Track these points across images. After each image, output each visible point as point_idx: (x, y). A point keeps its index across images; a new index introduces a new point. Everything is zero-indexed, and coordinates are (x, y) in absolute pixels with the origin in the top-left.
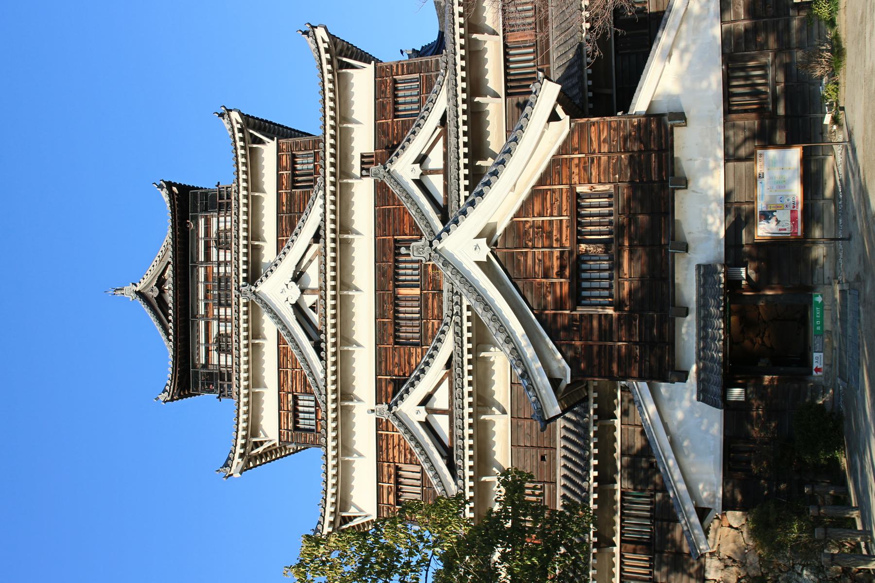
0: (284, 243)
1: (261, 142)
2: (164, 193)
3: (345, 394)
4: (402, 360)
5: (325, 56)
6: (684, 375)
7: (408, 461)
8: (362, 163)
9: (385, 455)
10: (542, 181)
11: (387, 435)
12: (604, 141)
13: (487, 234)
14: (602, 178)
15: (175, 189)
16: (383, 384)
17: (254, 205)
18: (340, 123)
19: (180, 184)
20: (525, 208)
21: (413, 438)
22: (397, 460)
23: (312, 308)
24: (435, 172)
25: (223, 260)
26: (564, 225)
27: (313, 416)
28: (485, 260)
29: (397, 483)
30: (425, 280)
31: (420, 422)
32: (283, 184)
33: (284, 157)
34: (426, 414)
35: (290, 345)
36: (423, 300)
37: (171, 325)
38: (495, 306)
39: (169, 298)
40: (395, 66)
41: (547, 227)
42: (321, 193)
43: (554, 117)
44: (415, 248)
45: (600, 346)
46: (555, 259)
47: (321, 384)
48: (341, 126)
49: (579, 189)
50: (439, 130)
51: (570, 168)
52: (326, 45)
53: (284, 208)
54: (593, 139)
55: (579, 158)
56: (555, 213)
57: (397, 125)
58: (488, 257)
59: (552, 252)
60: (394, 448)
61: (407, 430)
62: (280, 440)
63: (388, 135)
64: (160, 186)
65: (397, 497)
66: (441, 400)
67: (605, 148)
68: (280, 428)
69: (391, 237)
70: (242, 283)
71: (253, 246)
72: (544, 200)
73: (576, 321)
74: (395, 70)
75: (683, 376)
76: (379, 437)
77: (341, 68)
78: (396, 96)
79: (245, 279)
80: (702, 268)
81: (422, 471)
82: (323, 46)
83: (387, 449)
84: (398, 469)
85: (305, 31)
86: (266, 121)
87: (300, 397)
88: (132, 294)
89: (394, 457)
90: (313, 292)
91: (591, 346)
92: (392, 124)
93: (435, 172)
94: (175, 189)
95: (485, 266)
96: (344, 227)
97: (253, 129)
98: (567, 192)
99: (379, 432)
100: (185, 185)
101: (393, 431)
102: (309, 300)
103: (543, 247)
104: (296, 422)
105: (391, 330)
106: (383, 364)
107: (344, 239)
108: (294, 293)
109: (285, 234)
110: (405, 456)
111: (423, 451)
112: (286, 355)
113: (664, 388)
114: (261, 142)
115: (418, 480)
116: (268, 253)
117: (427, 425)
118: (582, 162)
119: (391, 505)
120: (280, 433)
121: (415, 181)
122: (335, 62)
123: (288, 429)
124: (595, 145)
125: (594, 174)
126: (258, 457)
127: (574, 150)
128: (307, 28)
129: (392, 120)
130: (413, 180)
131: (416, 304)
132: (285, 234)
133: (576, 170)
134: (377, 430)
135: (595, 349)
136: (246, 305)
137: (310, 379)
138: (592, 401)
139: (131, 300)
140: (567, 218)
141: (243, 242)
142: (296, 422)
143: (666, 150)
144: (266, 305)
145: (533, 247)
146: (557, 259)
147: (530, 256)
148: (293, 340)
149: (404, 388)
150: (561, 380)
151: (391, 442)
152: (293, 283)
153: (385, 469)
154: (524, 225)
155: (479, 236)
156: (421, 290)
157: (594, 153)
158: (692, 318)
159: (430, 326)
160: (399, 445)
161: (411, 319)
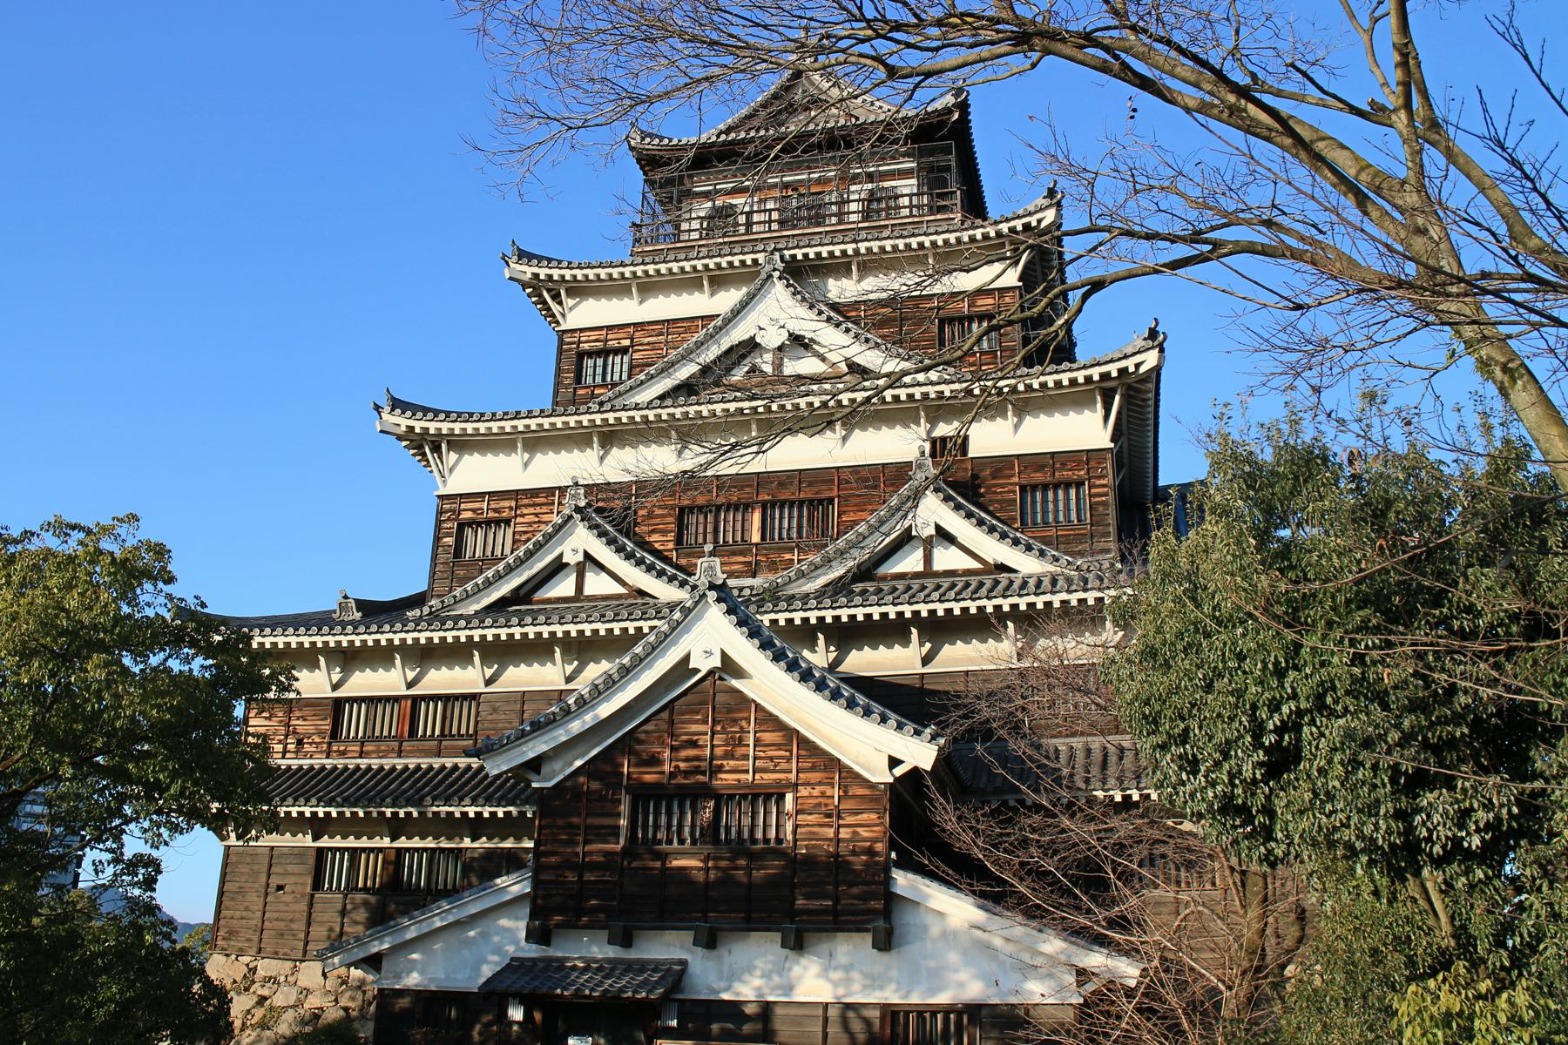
2: (949, 100)
3: (610, 438)
4: (658, 521)
7: (517, 537)
9: (526, 501)
10: (804, 743)
12: (855, 833)
13: (729, 666)
14: (803, 830)
19: (970, 121)
20: (769, 721)
21: (539, 546)
22: (519, 520)
23: (754, 369)
26: (742, 776)
27: (599, 379)
28: (691, 666)
29: (488, 522)
30: (771, 549)
31: (561, 555)
33: (991, 301)
37: (742, 135)
38: (629, 682)
41: (740, 751)
43: (894, 762)
45: (578, 827)
47: (618, 403)
49: (789, 797)
51: (820, 783)
52: (1132, 369)
54: (860, 817)
57: (1009, 492)
58: (697, 671)
60: (536, 515)
61: (549, 538)
63: (994, 478)
65: (470, 523)
66: (597, 584)
67: (844, 833)
68: (582, 330)
69: (835, 493)
70: (787, 253)
71: (849, 264)
72: (778, 746)
74: (1098, 482)
76: (550, 491)
78: (1056, 486)
80: (679, 968)
84: (507, 522)
87: (626, 359)
89: (523, 516)
92: (1011, 484)
93: (928, 559)
95: (683, 668)
96: (856, 418)
98: (787, 779)
102: (766, 364)
103: (713, 747)
104: (591, 354)
108: (773, 338)
110: (525, 532)
116: (841, 289)
117: (558, 567)
118: (829, 801)
120: (574, 331)
124: (849, 820)
125: (810, 817)
127: (844, 788)
129: (1016, 484)
133: (816, 792)
135: (575, 820)
136: (755, 261)
140: (750, 779)
143: (835, 921)
150: (539, 773)
153: (506, 504)
154: (745, 719)
155: (724, 655)
156: (756, 544)
158: (612, 952)
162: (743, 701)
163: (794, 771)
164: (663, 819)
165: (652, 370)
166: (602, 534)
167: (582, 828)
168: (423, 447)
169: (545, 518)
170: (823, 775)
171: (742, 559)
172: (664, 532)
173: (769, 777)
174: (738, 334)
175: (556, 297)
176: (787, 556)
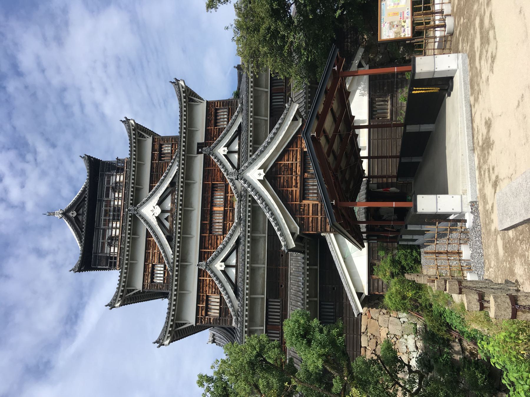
1: (143, 137)
4: (213, 241)
7: (213, 293)
9: (201, 290)
11: (203, 279)
16: (203, 253)
17: (139, 167)
20: (281, 158)
21: (218, 279)
23: (167, 219)
24: (235, 152)
25: (117, 196)
26: (298, 165)
28: (263, 179)
32: (154, 158)
34: (225, 266)
35: (154, 238)
36: (225, 213)
40: (216, 103)
43: (295, 119)
44: (231, 174)
45: (313, 218)
48: (189, 129)
50: (236, 133)
52: (184, 89)
56: (294, 160)
59: (292, 177)
61: (215, 275)
62: (143, 288)
69: (210, 183)
73: (302, 207)
74: (216, 104)
76: (199, 281)
77: (189, 101)
79: (131, 204)
81: (221, 298)
82: (182, 90)
83: (203, 287)
84: (208, 297)
88: (60, 215)
89: (206, 291)
90: (167, 211)
93: (235, 152)
97: (140, 130)
101: (207, 277)
103: (288, 175)
105: (208, 227)
107: (187, 183)
108: (158, 211)
111: (223, 286)
112: (149, 244)
115: (218, 302)
117: (224, 272)
119: (203, 316)
120: (143, 285)
121: (224, 155)
122: (187, 98)
123: (148, 282)
126: (129, 299)
128: (174, 81)
129: (214, 128)
130: (224, 155)
131: (222, 215)
135: (311, 219)
136: (130, 217)
139: (59, 218)
142: (152, 278)
144: (143, 218)
145: (284, 175)
146: (294, 180)
147: (282, 178)
151: (205, 283)
152: (157, 206)
154: (280, 165)
155: (260, 169)
156: (225, 207)
159: (228, 225)
160: (209, 285)
161: (218, 223)
162: (275, 164)
165: (161, 251)
166: (216, 256)
167: (314, 216)
168: (176, 332)
169: (208, 282)
170: (298, 140)
171: (229, 212)
172: (217, 239)
173: (299, 157)
175: (129, 291)
176: (229, 198)
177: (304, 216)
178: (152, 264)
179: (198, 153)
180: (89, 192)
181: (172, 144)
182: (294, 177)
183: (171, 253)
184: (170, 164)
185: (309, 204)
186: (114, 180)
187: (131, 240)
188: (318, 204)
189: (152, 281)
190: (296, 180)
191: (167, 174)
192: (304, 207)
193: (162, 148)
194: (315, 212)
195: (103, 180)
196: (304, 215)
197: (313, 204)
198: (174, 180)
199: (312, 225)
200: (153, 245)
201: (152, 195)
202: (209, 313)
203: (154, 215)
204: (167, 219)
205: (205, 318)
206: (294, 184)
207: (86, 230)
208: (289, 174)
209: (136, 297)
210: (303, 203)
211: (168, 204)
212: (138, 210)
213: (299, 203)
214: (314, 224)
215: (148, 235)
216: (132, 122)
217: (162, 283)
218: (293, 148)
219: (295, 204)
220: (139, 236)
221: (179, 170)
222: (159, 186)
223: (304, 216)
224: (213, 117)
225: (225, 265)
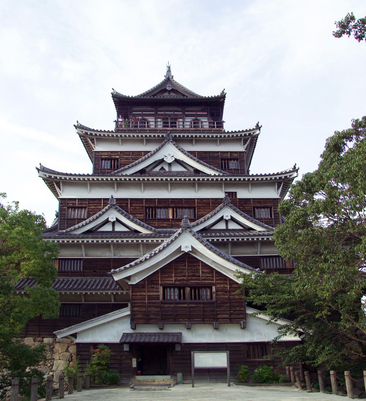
0: (194, 155)
1: (245, 143)
3: (121, 184)
5: (283, 176)
6: (134, 328)
8: (232, 193)
9: (91, 202)
10: (217, 272)
11: (101, 203)
15: (222, 100)
17: (213, 141)
18: (251, 183)
19: (224, 102)
21: (100, 215)
23: (162, 168)
32: (223, 154)
33: (236, 155)
35: (144, 158)
39: (166, 95)
42: (217, 174)
45: (145, 296)
46: (183, 278)
49: (214, 288)
52: (288, 177)
53: (211, 155)
55: (227, 287)
56: (203, 278)
59: (186, 277)
61: (104, 213)
64: (223, 92)
72: (209, 273)
73: (156, 286)
75: (134, 327)
77: (278, 182)
84: (85, 208)
85: (296, 167)
86: (255, 146)
89: (90, 206)
91: (145, 292)
94: (222, 100)
97: (251, 140)
99: (102, 200)
100: (224, 104)
106: (135, 202)
108: (169, 160)
109: (199, 155)
111: (94, 220)
113: (128, 321)
114: (245, 143)
118: (226, 289)
119: (67, 205)
122: (281, 180)
123: (101, 155)
132: (199, 155)
134: (104, 199)
135: (144, 294)
137: (127, 167)
138: (122, 292)
141: (194, 135)
142: (105, 159)
144: (162, 146)
146: (183, 279)
148: (146, 159)
149: (124, 211)
151: (98, 205)
152: (174, 159)
153: (85, 202)
157: (229, 293)
163: (215, 280)
164: (172, 294)
165: (130, 165)
166: (122, 214)
167: (147, 297)
174: (158, 157)
177: (146, 288)
178: (118, 158)
179: (226, 193)
180: (190, 99)
181: (238, 170)
182: (185, 278)
183: (128, 174)
184: (216, 169)
185: (159, 292)
186: (203, 120)
187: (141, 138)
188: (159, 299)
189: (102, 159)
190: (183, 280)
191: (207, 166)
192: (156, 288)
193: (234, 160)
194: (150, 297)
195: (203, 110)
196: (148, 288)
197: (159, 295)
198: (200, 173)
199: (138, 296)
200: (137, 158)
201: (185, 154)
202: (70, 209)
203: (165, 156)
204: (162, 168)
205: (65, 206)
206: (178, 278)
207: (155, 100)
208: (189, 274)
209: (89, 146)
210: (159, 287)
211: (177, 168)
212: (170, 143)
213: (160, 283)
214: (139, 297)
215: (147, 152)
216: (258, 132)
217: (101, 167)
218: (216, 276)
219: (159, 280)
220: (146, 145)
221: (210, 175)
222: (194, 160)
223: (146, 288)
224: (262, 206)
225: (110, 221)
